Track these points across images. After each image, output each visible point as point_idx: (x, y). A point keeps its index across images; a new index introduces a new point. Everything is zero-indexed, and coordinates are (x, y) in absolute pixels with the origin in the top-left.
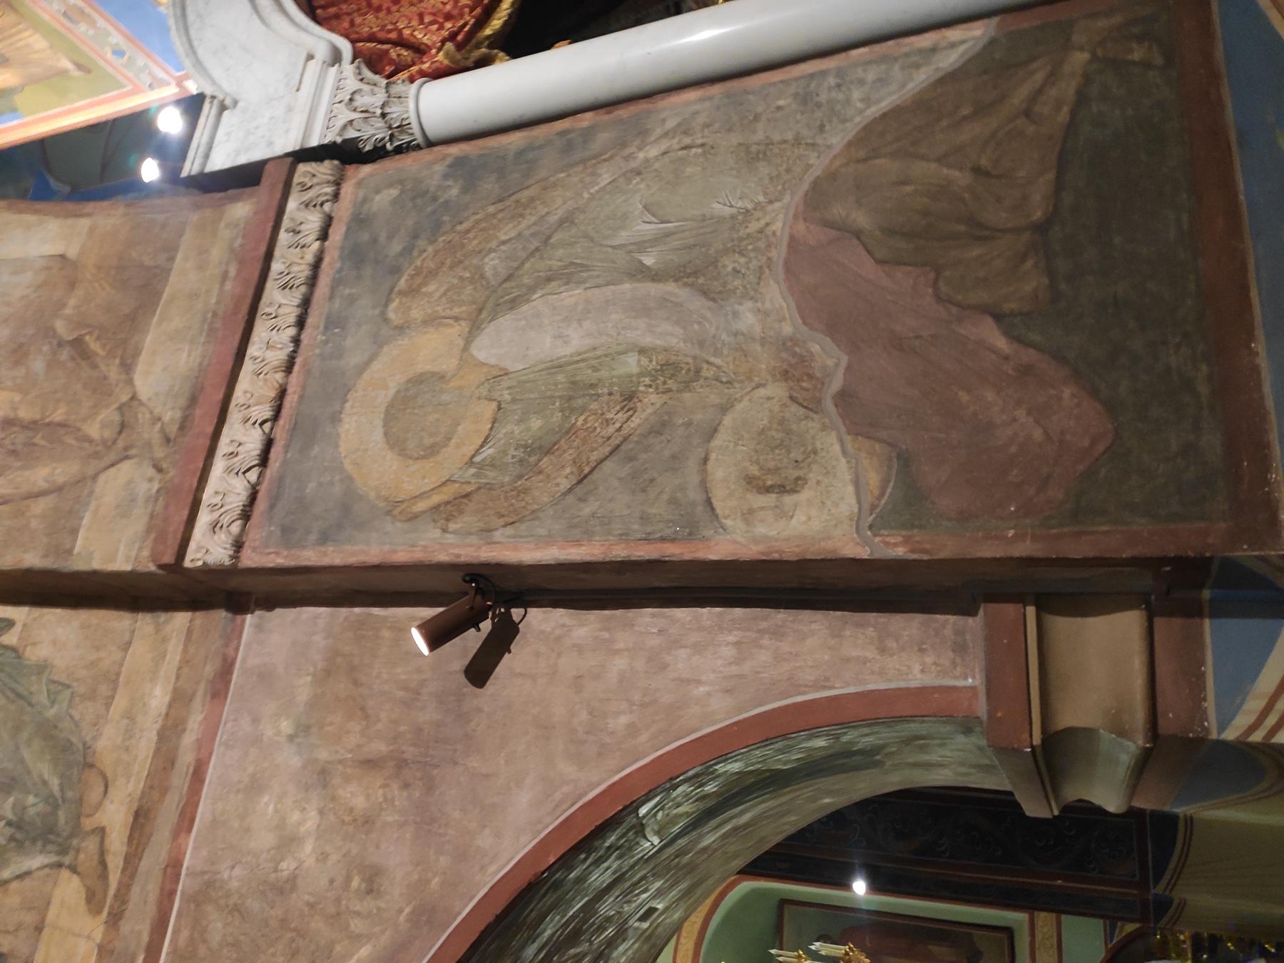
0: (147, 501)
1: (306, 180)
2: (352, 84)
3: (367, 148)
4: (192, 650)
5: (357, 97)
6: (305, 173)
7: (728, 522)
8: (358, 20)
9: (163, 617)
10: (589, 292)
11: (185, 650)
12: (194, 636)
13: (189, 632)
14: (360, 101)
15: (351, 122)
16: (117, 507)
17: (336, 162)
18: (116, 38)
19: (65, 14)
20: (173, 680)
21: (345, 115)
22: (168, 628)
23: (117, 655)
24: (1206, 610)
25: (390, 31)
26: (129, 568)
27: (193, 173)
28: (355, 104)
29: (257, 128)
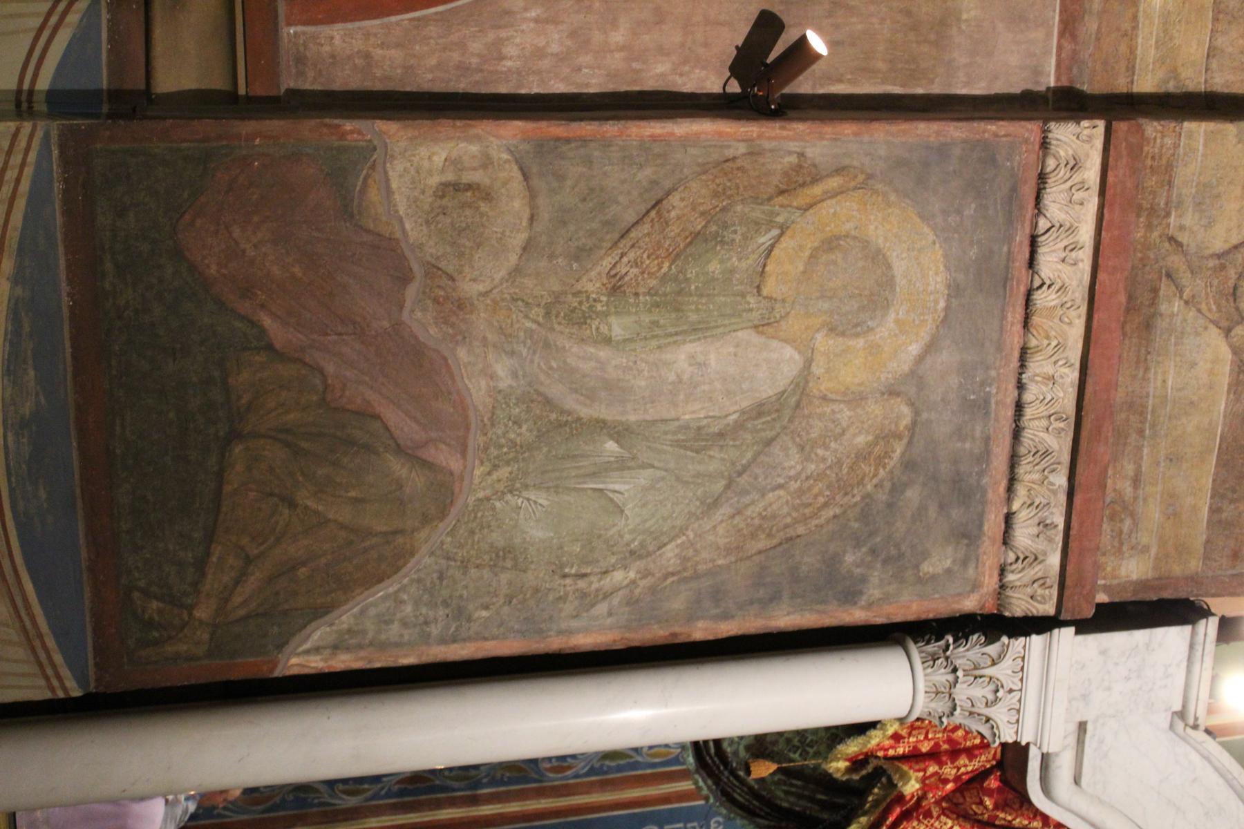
0: (1180, 204)
1: (1040, 591)
2: (1000, 714)
3: (975, 637)
4: (1123, 48)
5: (991, 697)
6: (1043, 601)
7: (505, 156)
9: (1171, 87)
10: (673, 414)
11: (1132, 50)
12: (1123, 65)
13: (1131, 69)
14: (980, 692)
15: (994, 663)
16: (1218, 196)
17: (1007, 614)
20: (1141, 14)
21: (1004, 671)
22: (1161, 74)
23: (1220, 41)
24: (105, 94)
26: (1186, 124)
27: (1203, 622)
28: (992, 687)
29: (1128, 679)
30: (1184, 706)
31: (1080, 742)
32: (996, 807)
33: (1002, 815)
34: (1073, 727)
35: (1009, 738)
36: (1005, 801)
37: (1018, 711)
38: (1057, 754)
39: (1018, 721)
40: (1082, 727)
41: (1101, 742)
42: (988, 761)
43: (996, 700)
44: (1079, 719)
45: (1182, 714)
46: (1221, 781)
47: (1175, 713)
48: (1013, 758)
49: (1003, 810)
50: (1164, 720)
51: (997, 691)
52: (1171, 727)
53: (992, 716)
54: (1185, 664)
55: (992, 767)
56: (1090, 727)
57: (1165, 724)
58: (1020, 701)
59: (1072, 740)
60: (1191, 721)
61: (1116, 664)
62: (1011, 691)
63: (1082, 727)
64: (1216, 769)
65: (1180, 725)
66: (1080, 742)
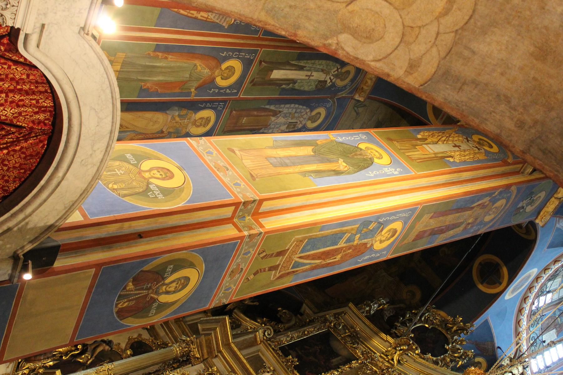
2: (7, 14)
5: (4, 6)
8: (24, 77)
18: (207, 158)
19: (228, 170)
25: (5, 64)
29: (64, 11)
30: (85, 26)
31: (42, 31)
32: (5, 50)
33: (8, 54)
34: (39, 25)
35: (10, 23)
36: (10, 49)
37: (15, 15)
38: (31, 35)
39: (15, 19)
40: (43, 26)
41: (50, 33)
42: (4, 32)
43: (6, 8)
44: (42, 22)
45: (83, 29)
46: (95, 56)
47: (81, 28)
48: (14, 33)
49: (8, 52)
50: (77, 30)
51: (7, 5)
52: (79, 33)
53: (4, 14)
54: (87, 10)
55: (6, 35)
56: (46, 26)
57: (77, 31)
58: (17, 11)
59: (38, 30)
60: (86, 32)
61: (60, 4)
62: (13, 6)
63: (43, 26)
64: (94, 51)
65: (82, 32)
66: (42, 31)
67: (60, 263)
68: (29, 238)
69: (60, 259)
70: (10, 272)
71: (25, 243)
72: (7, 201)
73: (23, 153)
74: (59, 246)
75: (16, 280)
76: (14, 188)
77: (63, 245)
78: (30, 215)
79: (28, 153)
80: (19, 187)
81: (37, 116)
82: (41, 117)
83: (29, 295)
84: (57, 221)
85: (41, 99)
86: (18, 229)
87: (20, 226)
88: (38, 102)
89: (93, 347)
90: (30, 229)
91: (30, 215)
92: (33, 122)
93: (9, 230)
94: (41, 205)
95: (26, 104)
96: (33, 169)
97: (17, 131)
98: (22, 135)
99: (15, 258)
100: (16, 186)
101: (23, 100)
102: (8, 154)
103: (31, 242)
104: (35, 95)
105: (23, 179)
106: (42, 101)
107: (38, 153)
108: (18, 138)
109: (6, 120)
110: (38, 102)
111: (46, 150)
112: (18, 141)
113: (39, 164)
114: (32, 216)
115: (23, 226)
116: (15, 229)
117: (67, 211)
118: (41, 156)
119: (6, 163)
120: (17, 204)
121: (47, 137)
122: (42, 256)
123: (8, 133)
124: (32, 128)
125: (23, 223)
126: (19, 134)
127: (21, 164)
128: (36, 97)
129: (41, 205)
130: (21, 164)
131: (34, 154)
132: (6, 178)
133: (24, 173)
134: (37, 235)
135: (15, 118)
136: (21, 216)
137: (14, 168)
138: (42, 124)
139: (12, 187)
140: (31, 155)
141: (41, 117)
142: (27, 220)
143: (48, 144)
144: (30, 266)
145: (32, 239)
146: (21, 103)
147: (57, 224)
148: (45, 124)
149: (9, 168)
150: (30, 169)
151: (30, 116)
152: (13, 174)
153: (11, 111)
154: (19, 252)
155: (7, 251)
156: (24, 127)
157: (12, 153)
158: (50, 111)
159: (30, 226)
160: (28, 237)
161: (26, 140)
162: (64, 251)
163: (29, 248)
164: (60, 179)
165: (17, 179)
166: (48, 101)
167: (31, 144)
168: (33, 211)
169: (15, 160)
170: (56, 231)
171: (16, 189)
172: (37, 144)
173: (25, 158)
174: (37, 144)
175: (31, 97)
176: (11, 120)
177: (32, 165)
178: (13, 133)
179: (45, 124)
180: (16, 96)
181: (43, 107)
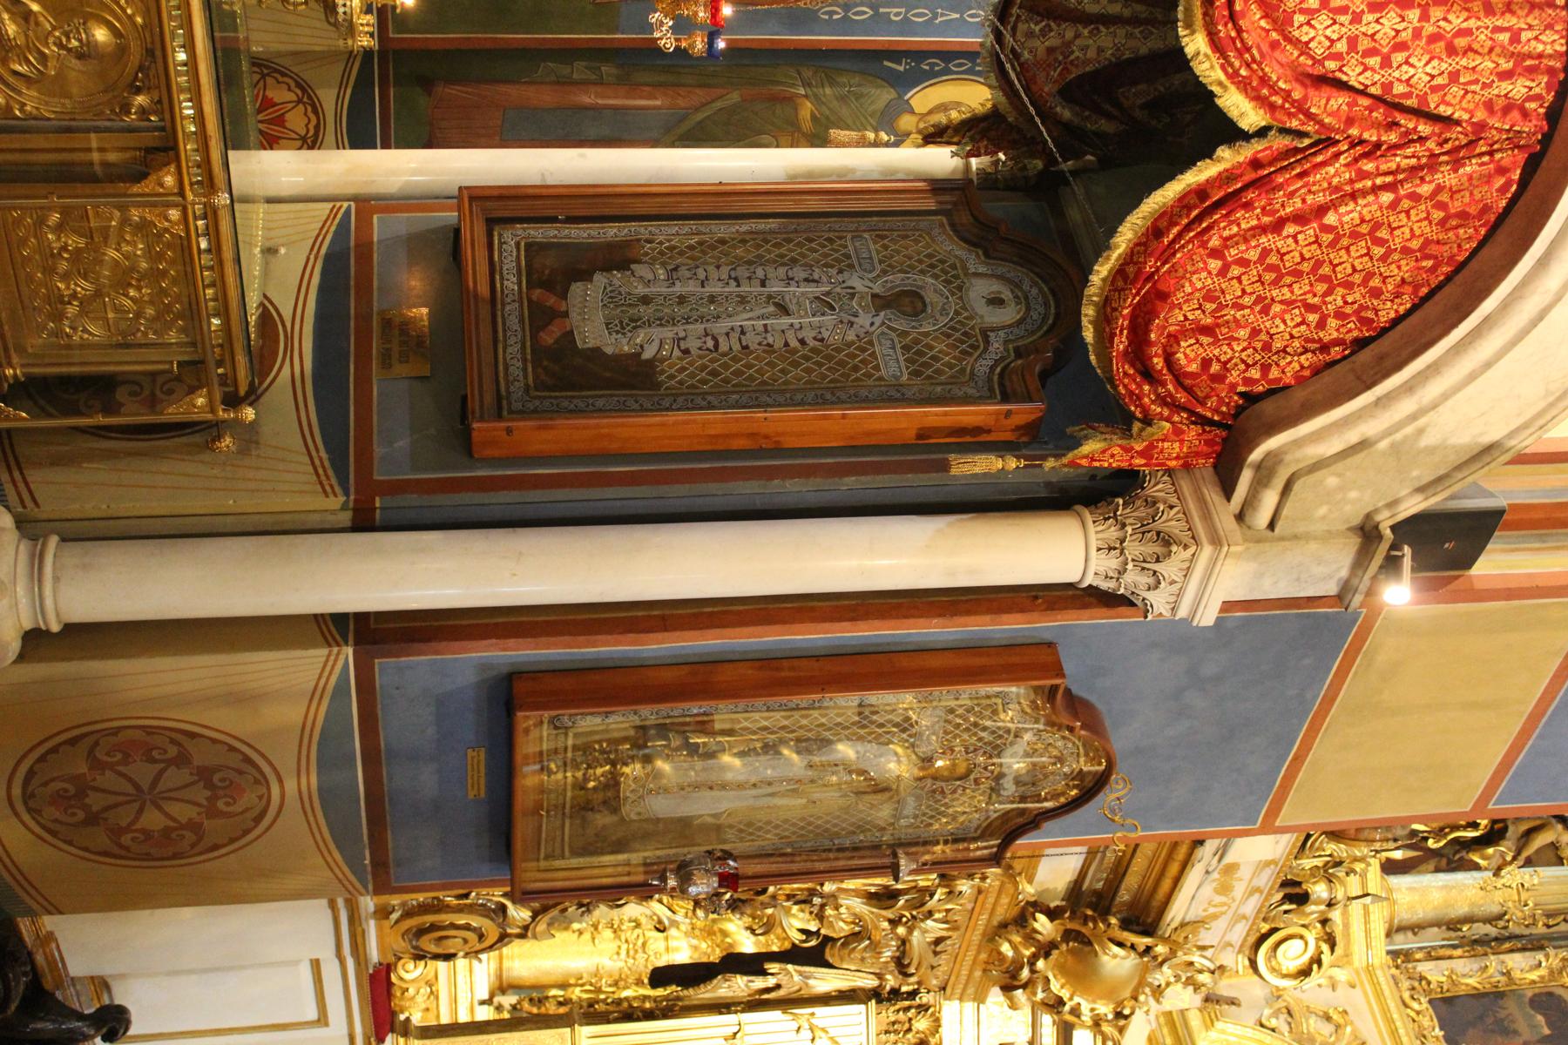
67: (1494, 563)
68: (1418, 478)
69: (1494, 551)
70: (1344, 573)
71: (1404, 493)
72: (1365, 355)
73: (1441, 206)
74: (1499, 513)
75: (1357, 600)
76: (1392, 315)
77: (1514, 507)
78: (1434, 406)
79: (1456, 206)
80: (1409, 313)
81: (1505, 86)
82: (1518, 89)
83: (1382, 648)
84: (1511, 435)
85: (1530, 27)
86: (1393, 446)
87: (1398, 436)
88: (1515, 38)
89: (1524, 827)
90: (1426, 447)
91: (1434, 406)
92: (1489, 106)
93: (1363, 445)
94: (1472, 377)
95: (1476, 46)
96: (1460, 258)
97: (1433, 133)
98: (1447, 147)
99: (1367, 533)
100: (1402, 310)
101: (1468, 32)
102: (1393, 206)
103: (1420, 490)
104: (1513, 13)
105: (1425, 290)
106: (1530, 34)
107: (1486, 209)
108: (1433, 156)
109: (1408, 95)
110: (1515, 38)
111: (1513, 201)
112: (1433, 163)
113: (1481, 244)
114: (1440, 409)
115: (1406, 438)
116: (1383, 445)
117: (1551, 405)
118: (1493, 218)
119: (1383, 233)
120: (1399, 367)
121: (1521, 157)
122: (1446, 539)
123: (1408, 139)
124: (1481, 127)
125: (1409, 430)
126: (1441, 145)
127: (1427, 242)
128: (1514, 21)
129: (1472, 377)
130: (1427, 242)
131: (1473, 210)
132: (1375, 282)
133: (1433, 270)
134: (1442, 472)
135: (1435, 89)
136: (1407, 406)
137: (1406, 251)
138: (1515, 115)
139: (1387, 312)
140: (1463, 215)
141: (1518, 89)
142: (1421, 422)
143: (1524, 183)
144: (1407, 562)
145: (1424, 481)
146: (1461, 42)
147: (1513, 443)
148: (1525, 114)
149: (1389, 252)
150: (1451, 258)
151: (1485, 86)
152: (1404, 268)
153: (1428, 69)
154: (1378, 518)
155: (1348, 508)
156: (1458, 123)
157: (1406, 204)
158: (1551, 71)
159: (1424, 442)
160: (1415, 473)
161: (1457, 164)
162: (1511, 526)
163: (1413, 506)
164: (1548, 299)
165: (1408, 289)
166: (1548, 37)
167: (1470, 178)
168: (1445, 397)
169: (1413, 226)
170: (1509, 463)
171: (1395, 322)
172: (1488, 179)
173: (1442, 223)
174: (1488, 179)
175: (1499, 23)
176: (1423, 99)
177: (1459, 246)
178: (1422, 140)
179: (1525, 114)
180: (1451, 17)
181: (1530, 56)
